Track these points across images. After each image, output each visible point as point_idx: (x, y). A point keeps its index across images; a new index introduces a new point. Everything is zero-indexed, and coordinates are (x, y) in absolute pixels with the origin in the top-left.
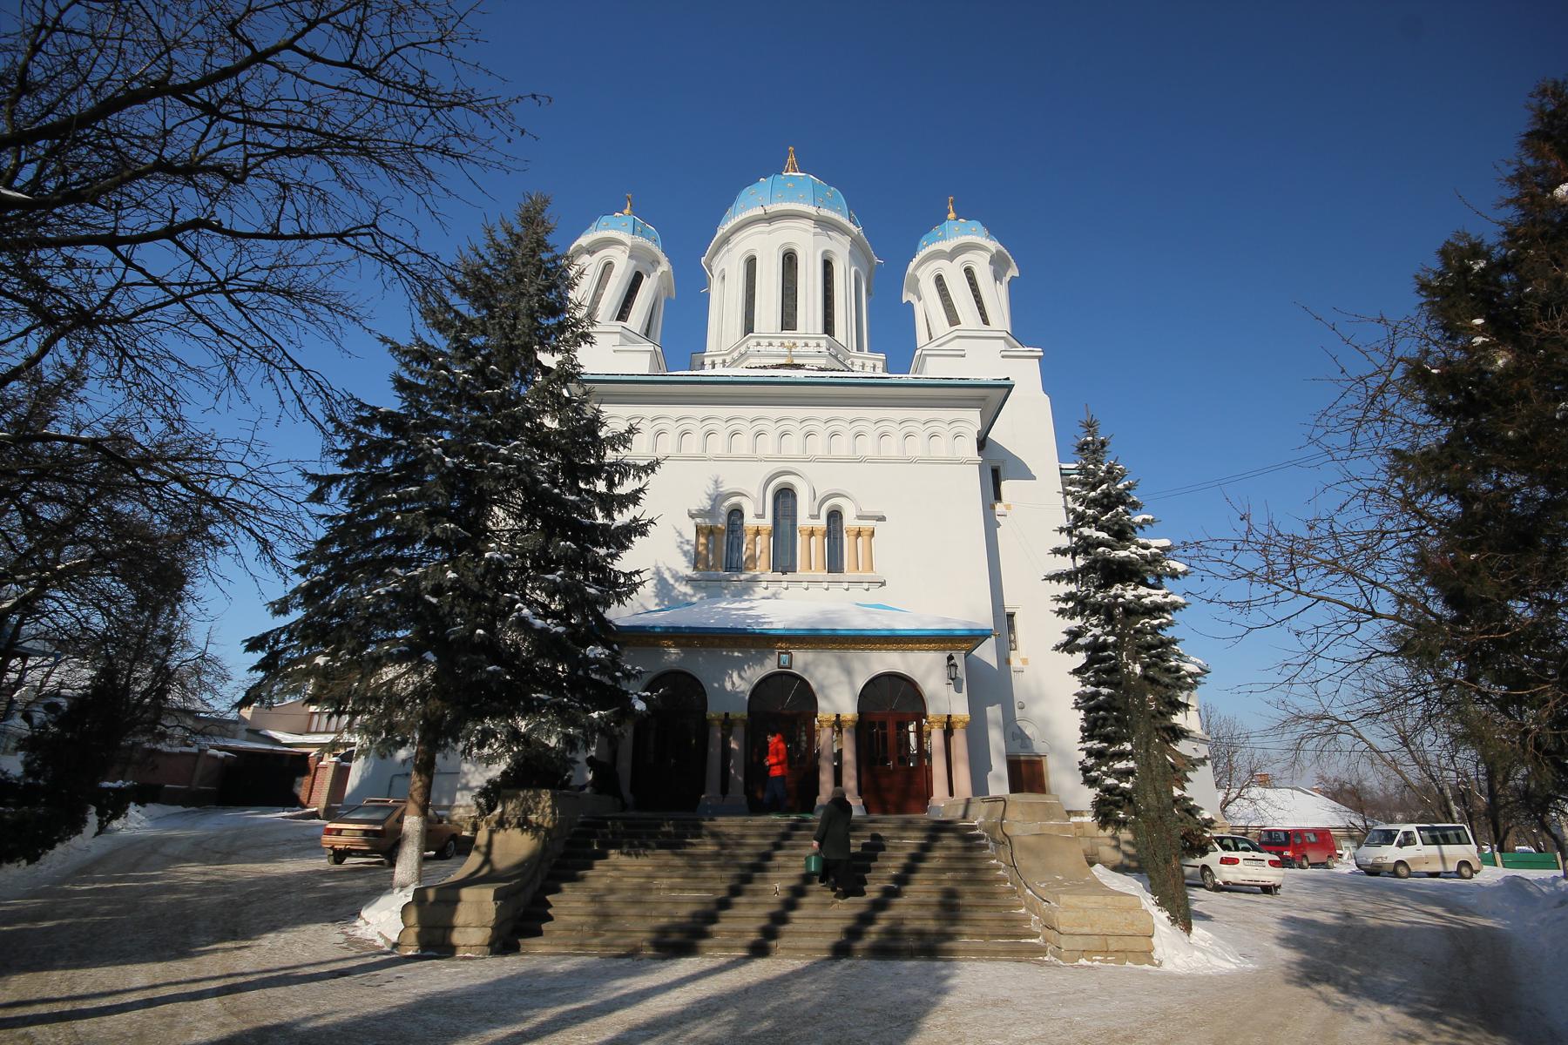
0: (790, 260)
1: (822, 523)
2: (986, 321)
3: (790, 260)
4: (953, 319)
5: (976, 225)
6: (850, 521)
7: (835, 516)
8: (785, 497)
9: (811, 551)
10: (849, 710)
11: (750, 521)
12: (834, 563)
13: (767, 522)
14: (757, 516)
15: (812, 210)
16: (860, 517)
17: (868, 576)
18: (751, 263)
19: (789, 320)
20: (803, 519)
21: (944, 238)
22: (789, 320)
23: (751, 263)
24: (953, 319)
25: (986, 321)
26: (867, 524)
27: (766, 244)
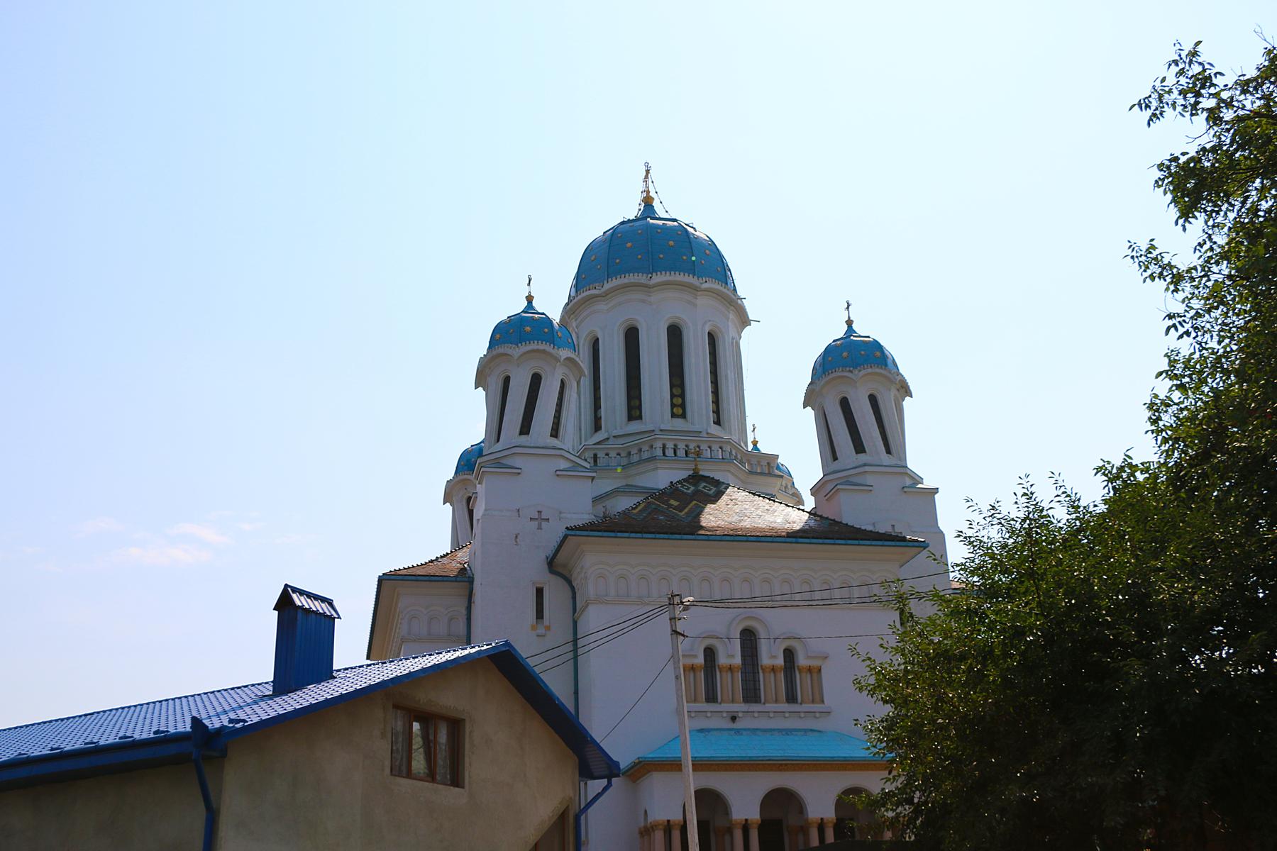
0: (675, 335)
1: (780, 661)
3: (675, 335)
4: (859, 447)
6: (802, 661)
7: (789, 654)
8: (749, 639)
9: (771, 684)
11: (722, 660)
13: (738, 660)
14: (730, 655)
16: (809, 657)
18: (632, 337)
19: (679, 407)
24: (859, 447)
26: (814, 663)
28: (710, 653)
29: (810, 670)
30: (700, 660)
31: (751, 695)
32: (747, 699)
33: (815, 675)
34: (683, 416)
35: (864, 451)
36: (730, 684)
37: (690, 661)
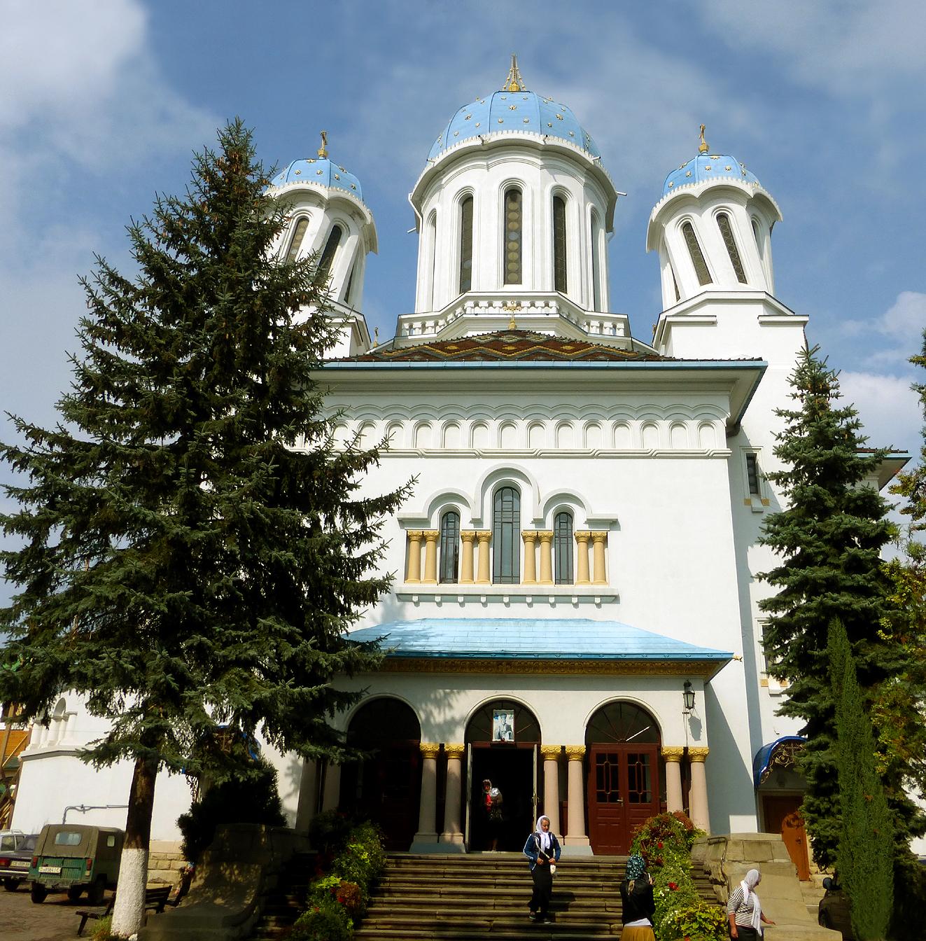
2: (742, 278)
4: (704, 276)
5: (726, 161)
6: (579, 524)
7: (564, 517)
9: (535, 563)
10: (576, 741)
11: (465, 525)
12: (564, 574)
15: (538, 139)
17: (600, 589)
18: (467, 201)
19: (512, 271)
20: (526, 525)
21: (691, 179)
22: (512, 271)
23: (467, 201)
24: (704, 276)
25: (742, 278)
26: (599, 532)
27: (484, 183)
28: (450, 517)
29: (590, 540)
30: (435, 524)
31: (505, 571)
32: (499, 578)
33: (598, 545)
34: (519, 282)
35: (711, 281)
36: (476, 562)
37: (416, 531)
